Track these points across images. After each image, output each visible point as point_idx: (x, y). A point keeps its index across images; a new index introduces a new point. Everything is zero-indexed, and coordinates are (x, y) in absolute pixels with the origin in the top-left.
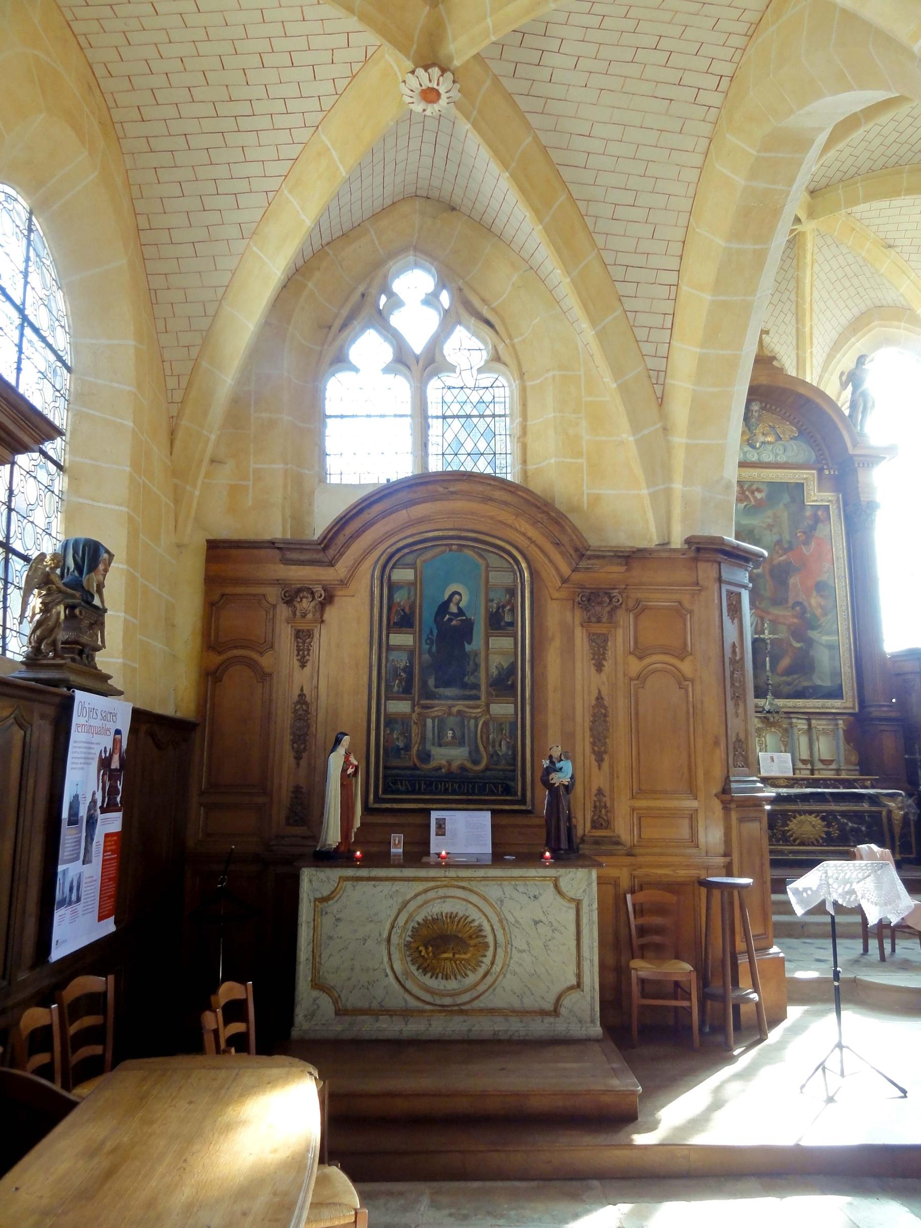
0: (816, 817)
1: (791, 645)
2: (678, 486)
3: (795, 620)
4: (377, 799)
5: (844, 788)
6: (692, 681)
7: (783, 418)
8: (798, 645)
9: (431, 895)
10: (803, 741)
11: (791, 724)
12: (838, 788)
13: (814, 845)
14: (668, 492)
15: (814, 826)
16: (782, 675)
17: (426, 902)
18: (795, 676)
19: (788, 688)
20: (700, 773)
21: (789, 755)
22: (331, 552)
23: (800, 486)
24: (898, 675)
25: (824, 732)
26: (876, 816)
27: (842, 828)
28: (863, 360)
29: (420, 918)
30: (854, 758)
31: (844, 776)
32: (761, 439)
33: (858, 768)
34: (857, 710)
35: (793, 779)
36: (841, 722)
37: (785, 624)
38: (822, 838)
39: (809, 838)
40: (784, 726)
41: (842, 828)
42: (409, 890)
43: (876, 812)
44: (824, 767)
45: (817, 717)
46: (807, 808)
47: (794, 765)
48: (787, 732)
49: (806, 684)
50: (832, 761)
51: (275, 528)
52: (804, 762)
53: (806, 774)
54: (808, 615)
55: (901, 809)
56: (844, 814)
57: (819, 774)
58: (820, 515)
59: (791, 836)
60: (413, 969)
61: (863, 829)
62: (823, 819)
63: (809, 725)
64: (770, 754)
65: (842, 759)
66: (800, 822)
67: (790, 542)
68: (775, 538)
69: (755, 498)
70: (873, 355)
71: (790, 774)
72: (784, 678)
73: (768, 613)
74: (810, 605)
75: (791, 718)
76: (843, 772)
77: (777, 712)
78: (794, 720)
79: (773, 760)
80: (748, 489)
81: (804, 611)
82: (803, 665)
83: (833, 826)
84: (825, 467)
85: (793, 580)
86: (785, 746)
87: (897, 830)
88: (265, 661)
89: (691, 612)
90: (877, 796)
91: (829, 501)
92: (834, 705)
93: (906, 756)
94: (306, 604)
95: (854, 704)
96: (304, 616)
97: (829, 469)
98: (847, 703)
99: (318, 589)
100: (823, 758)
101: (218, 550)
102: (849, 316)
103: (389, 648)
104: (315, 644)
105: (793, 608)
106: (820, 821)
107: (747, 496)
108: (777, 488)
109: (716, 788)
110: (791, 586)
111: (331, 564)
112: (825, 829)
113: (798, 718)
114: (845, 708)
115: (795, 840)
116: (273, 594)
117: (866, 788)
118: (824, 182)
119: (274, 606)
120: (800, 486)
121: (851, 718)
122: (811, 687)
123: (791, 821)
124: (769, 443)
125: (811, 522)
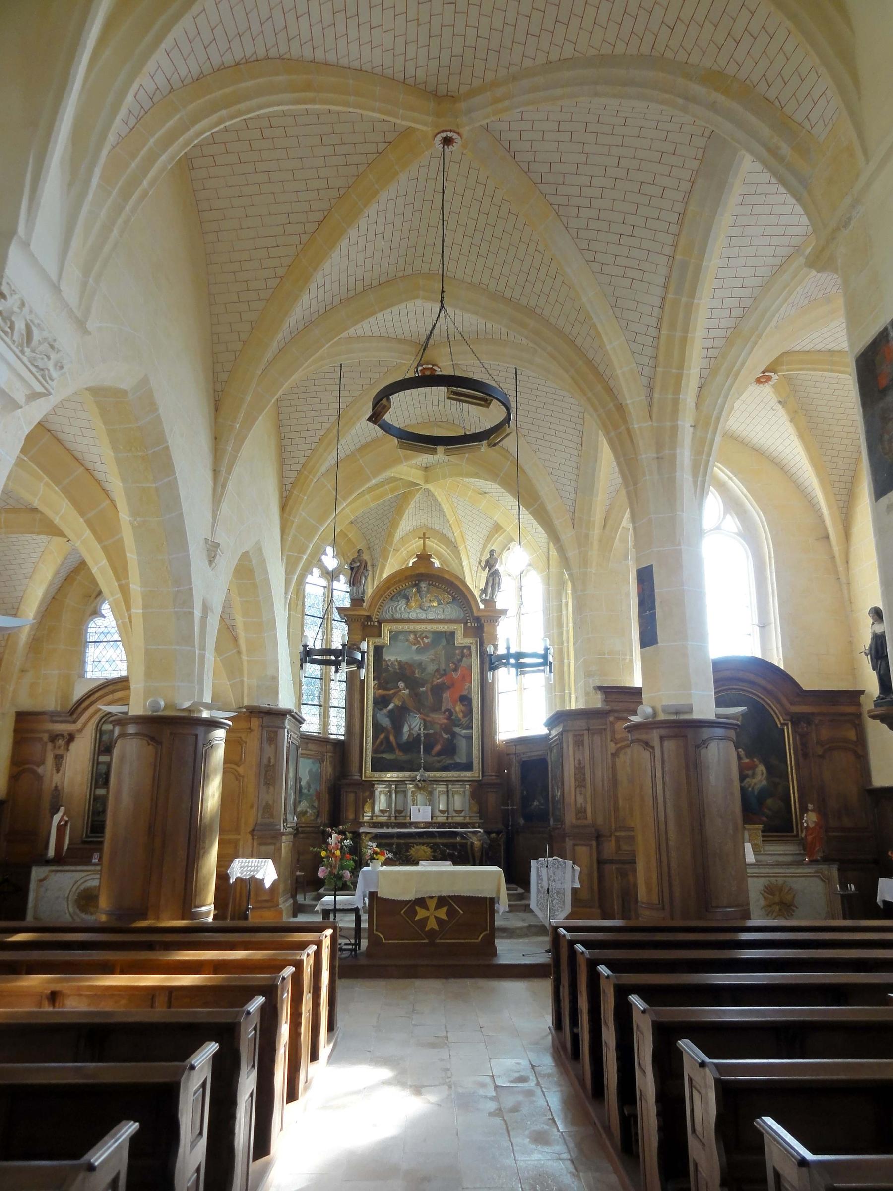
2: (245, 679)
3: (445, 721)
4: (87, 836)
6: (243, 777)
8: (446, 737)
9: (88, 878)
14: (242, 682)
17: (86, 881)
20: (243, 820)
22: (75, 716)
24: (508, 755)
25: (457, 792)
26: (464, 846)
29: (82, 888)
30: (476, 809)
31: (467, 820)
32: (427, 605)
36: (468, 786)
42: (78, 876)
46: (421, 841)
48: (431, 793)
49: (451, 762)
51: (50, 703)
52: (442, 812)
53: (441, 819)
55: (480, 840)
56: (445, 845)
58: (465, 651)
60: (78, 911)
62: (431, 847)
64: (418, 807)
65: (467, 809)
67: (444, 670)
68: (436, 667)
69: (424, 642)
71: (430, 820)
72: (436, 758)
77: (424, 780)
81: (451, 713)
82: (450, 749)
85: (446, 695)
87: (478, 854)
88: (40, 770)
89: (246, 743)
90: (466, 833)
92: (467, 775)
94: (60, 742)
96: (59, 748)
98: (474, 774)
99: (66, 735)
101: (23, 717)
103: (98, 763)
104: (64, 761)
105: (444, 712)
108: (438, 635)
109: (250, 829)
111: (75, 722)
116: (45, 737)
118: (429, 465)
119: (46, 744)
120: (453, 634)
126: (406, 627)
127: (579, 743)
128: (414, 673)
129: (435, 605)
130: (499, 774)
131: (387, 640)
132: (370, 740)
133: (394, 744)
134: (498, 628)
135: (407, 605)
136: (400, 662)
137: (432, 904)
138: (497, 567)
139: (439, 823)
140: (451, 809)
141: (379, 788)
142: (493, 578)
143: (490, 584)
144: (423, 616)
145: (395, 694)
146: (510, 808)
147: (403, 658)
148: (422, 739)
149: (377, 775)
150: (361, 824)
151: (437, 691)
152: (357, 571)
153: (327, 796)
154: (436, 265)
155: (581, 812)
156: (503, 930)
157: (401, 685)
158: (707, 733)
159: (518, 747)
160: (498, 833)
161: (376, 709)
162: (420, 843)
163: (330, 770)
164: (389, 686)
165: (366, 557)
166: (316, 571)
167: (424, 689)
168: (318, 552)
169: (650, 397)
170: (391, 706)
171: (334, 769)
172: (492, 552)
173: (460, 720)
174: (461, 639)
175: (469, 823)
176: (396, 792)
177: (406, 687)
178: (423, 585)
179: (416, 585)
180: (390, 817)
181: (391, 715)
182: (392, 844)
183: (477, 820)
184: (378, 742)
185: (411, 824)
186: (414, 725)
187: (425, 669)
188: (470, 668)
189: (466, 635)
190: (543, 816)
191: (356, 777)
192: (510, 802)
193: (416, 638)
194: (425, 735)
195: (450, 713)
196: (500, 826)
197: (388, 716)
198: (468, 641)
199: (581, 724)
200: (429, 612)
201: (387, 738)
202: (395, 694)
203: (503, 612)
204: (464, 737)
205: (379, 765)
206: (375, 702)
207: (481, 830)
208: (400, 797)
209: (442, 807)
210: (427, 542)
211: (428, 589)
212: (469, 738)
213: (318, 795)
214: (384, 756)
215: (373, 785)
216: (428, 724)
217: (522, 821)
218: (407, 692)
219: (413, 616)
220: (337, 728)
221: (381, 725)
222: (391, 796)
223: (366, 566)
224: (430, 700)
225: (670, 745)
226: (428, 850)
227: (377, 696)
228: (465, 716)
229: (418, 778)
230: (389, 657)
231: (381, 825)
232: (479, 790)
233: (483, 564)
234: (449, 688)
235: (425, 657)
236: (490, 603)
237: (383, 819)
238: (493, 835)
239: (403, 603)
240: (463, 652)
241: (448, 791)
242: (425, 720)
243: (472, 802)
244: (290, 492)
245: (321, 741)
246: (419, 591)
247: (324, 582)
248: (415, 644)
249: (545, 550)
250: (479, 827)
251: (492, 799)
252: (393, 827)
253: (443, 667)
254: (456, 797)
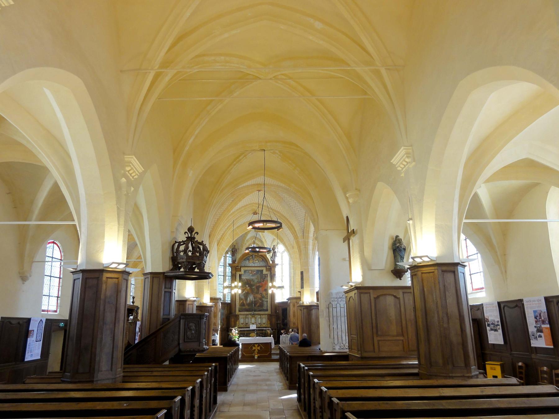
10: (260, 320)
26: (265, 333)
30: (269, 322)
58: (266, 276)
82: (262, 305)
85: (260, 289)
92: (267, 313)
98: (269, 312)
108: (258, 271)
120: (262, 271)
127: (294, 306)
130: (276, 312)
137: (256, 346)
141: (240, 317)
147: (248, 278)
149: (240, 313)
151: (258, 288)
152: (234, 251)
154: (257, 202)
155: (294, 324)
156: (274, 354)
158: (313, 307)
169: (303, 234)
174: (265, 272)
177: (249, 286)
183: (269, 326)
190: (287, 324)
198: (268, 273)
199: (295, 301)
200: (255, 264)
203: (277, 264)
212: (267, 302)
220: (228, 300)
224: (256, 291)
225: (305, 310)
230: (243, 277)
232: (270, 317)
236: (273, 261)
244: (219, 241)
245: (224, 304)
251: (274, 320)
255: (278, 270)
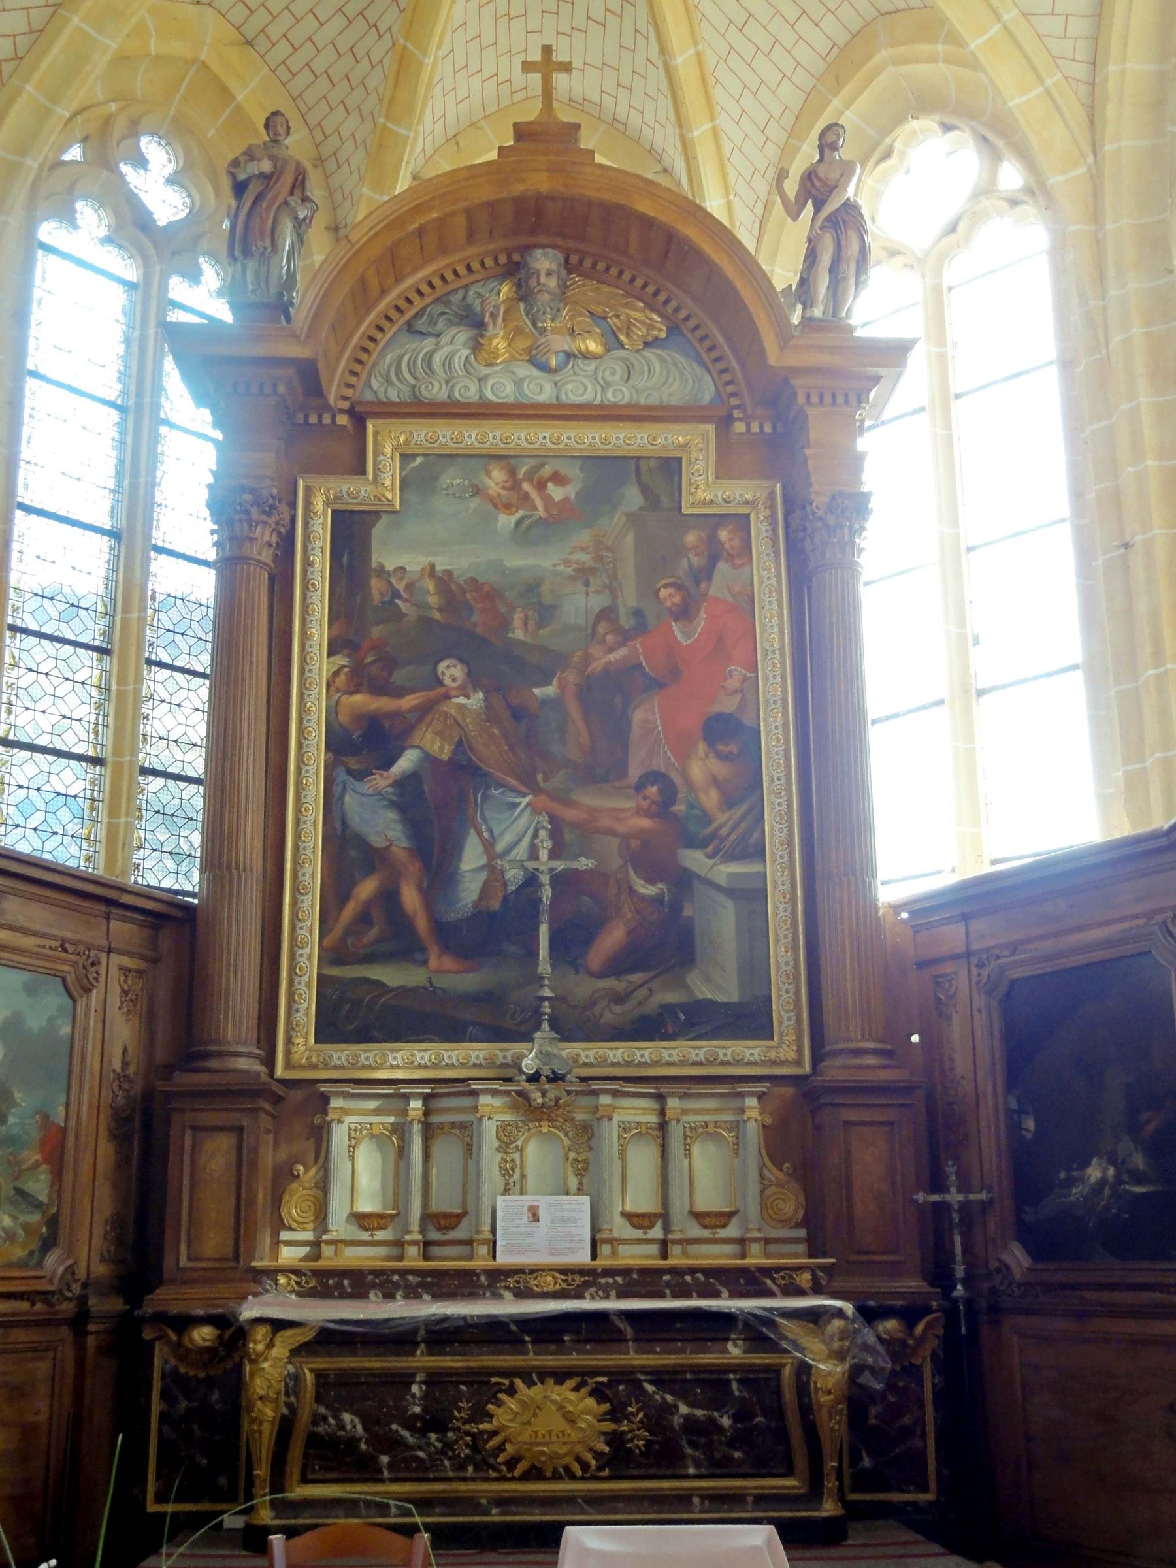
0: (576, 1389)
1: (631, 891)
3: (645, 823)
5: (734, 1295)
7: (628, 294)
10: (642, 1161)
11: (596, 1109)
12: (716, 1295)
13: (573, 1477)
15: (570, 1419)
16: (600, 975)
18: (637, 977)
19: (618, 1009)
21: (586, 1200)
23: (671, 467)
24: (921, 965)
25: (707, 1132)
26: (761, 1382)
27: (657, 1418)
28: (830, 137)
30: (791, 1205)
31: (756, 1258)
32: (560, 342)
33: (802, 1233)
34: (807, 1069)
35: (581, 1271)
36: (752, 1102)
37: (612, 833)
38: (598, 1455)
39: (553, 1456)
40: (579, 1116)
41: (657, 1418)
43: (767, 1368)
44: (706, 1233)
45: (680, 1088)
47: (595, 1229)
48: (586, 1133)
49: (671, 997)
50: (731, 1215)
53: (637, 1254)
54: (679, 808)
55: (840, 1356)
56: (662, 1378)
57: (685, 1254)
58: (724, 536)
59: (501, 1448)
61: (726, 1422)
62: (598, 1393)
63: (662, 1112)
64: (528, 1200)
66: (524, 1405)
67: (638, 613)
68: (598, 602)
69: (547, 499)
70: (888, 140)
71: (583, 1257)
73: (570, 804)
74: (688, 782)
75: (596, 1093)
76: (755, 1248)
77: (555, 1078)
78: (605, 1100)
79: (535, 1217)
80: (529, 477)
81: (669, 794)
82: (667, 944)
83: (628, 1417)
84: (736, 414)
85: (645, 715)
86: (580, 1174)
90: (766, 1320)
91: (747, 503)
92: (745, 1053)
93: (920, 1197)
95: (800, 1050)
97: (747, 420)
98: (783, 1049)
100: (702, 1206)
102: (823, 45)
105: (639, 787)
106: (591, 1402)
107: (526, 495)
108: (608, 470)
110: (636, 730)
112: (609, 1426)
113: (615, 1094)
114: (774, 1063)
115: (512, 1463)
117: (800, 1292)
120: (671, 467)
121: (788, 1091)
122: (681, 1006)
123: (499, 1403)
124: (586, 356)
125: (696, 561)
126: (471, 435)
128: (505, 624)
129: (593, 346)
131: (395, 498)
132: (312, 904)
133: (422, 923)
134: (862, 444)
135: (476, 346)
136: (444, 581)
138: (850, 192)
139: (626, 1272)
140: (679, 1207)
142: (838, 234)
143: (825, 259)
144: (542, 391)
145: (425, 710)
146: (954, 1197)
147: (459, 561)
148: (547, 893)
149: (340, 1054)
150: (261, 1277)
151: (610, 697)
153: (106, 1150)
157: (452, 672)
159: (977, 926)
160: (910, 1315)
161: (341, 775)
162: (544, 1375)
163: (123, 1032)
164: (399, 676)
165: (296, 145)
166: (91, 219)
167: (550, 690)
168: (109, 142)
170: (406, 762)
171: (150, 1018)
172: (828, 142)
173: (706, 818)
174: (705, 489)
175: (767, 1271)
176: (429, 1132)
177: (474, 681)
178: (545, 262)
179: (514, 269)
180: (399, 1244)
181: (408, 798)
182: (404, 1380)
184: (350, 910)
185: (498, 1279)
186: (506, 841)
187: (554, 607)
188: (744, 607)
189: (724, 471)
191: (242, 1064)
192: (951, 1170)
193: (515, 486)
194: (558, 880)
195: (664, 790)
196: (913, 1285)
197: (393, 804)
198: (741, 492)
201: (389, 897)
202: (425, 710)
204: (730, 892)
205: (348, 1016)
206: (340, 744)
207: (848, 1307)
208: (447, 1152)
209: (641, 1196)
210: (560, 80)
211: (564, 286)
212: (751, 896)
213: (55, 1148)
214: (375, 972)
215: (325, 1099)
216: (568, 836)
217: (1017, 1258)
218: (476, 701)
219: (501, 388)
221: (362, 843)
222: (402, 1152)
223: (299, 183)
226: (587, 1407)
227: (344, 718)
228: (729, 802)
229: (529, 1064)
230: (396, 555)
231: (358, 1283)
233: (791, 186)
234: (656, 685)
235: (546, 561)
236: (833, 324)
237: (362, 1257)
238: (890, 1325)
239: (454, 344)
240: (712, 539)
241: (663, 1126)
242: (553, 819)
243: (773, 1173)
246: (524, 294)
247: (130, 271)
248: (508, 507)
249: (1079, 71)
250: (817, 1290)
251: (871, 1160)
252: (412, 1293)
253: (629, 599)
254: (696, 1150)
255: (890, 456)
